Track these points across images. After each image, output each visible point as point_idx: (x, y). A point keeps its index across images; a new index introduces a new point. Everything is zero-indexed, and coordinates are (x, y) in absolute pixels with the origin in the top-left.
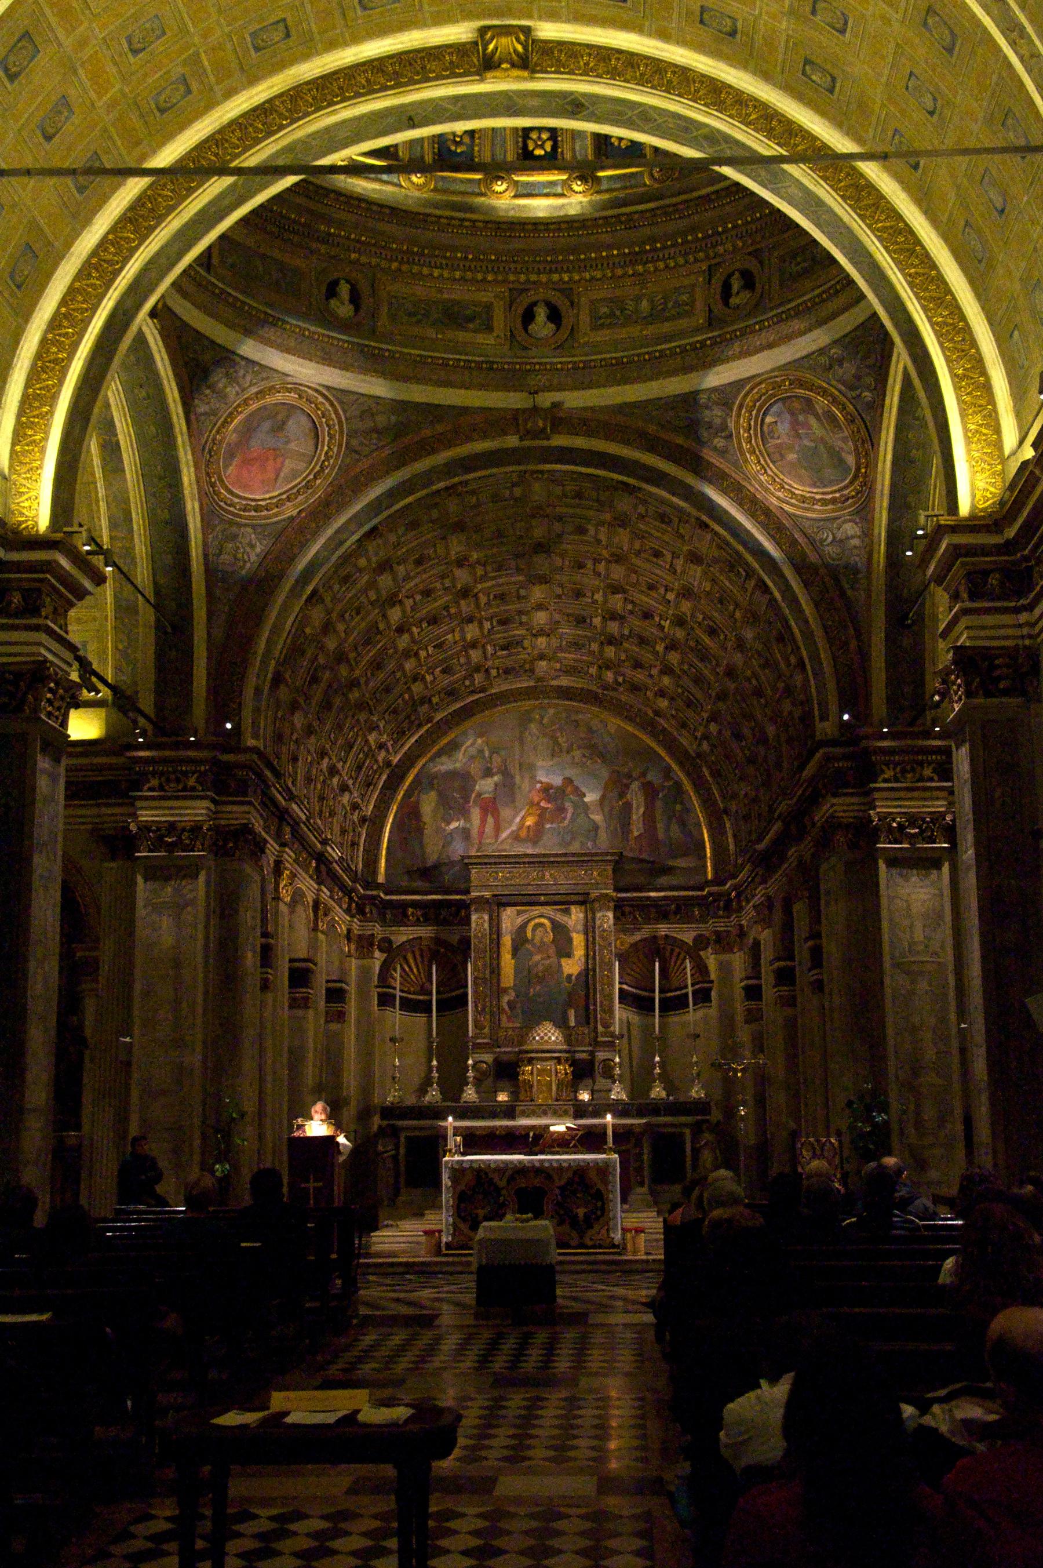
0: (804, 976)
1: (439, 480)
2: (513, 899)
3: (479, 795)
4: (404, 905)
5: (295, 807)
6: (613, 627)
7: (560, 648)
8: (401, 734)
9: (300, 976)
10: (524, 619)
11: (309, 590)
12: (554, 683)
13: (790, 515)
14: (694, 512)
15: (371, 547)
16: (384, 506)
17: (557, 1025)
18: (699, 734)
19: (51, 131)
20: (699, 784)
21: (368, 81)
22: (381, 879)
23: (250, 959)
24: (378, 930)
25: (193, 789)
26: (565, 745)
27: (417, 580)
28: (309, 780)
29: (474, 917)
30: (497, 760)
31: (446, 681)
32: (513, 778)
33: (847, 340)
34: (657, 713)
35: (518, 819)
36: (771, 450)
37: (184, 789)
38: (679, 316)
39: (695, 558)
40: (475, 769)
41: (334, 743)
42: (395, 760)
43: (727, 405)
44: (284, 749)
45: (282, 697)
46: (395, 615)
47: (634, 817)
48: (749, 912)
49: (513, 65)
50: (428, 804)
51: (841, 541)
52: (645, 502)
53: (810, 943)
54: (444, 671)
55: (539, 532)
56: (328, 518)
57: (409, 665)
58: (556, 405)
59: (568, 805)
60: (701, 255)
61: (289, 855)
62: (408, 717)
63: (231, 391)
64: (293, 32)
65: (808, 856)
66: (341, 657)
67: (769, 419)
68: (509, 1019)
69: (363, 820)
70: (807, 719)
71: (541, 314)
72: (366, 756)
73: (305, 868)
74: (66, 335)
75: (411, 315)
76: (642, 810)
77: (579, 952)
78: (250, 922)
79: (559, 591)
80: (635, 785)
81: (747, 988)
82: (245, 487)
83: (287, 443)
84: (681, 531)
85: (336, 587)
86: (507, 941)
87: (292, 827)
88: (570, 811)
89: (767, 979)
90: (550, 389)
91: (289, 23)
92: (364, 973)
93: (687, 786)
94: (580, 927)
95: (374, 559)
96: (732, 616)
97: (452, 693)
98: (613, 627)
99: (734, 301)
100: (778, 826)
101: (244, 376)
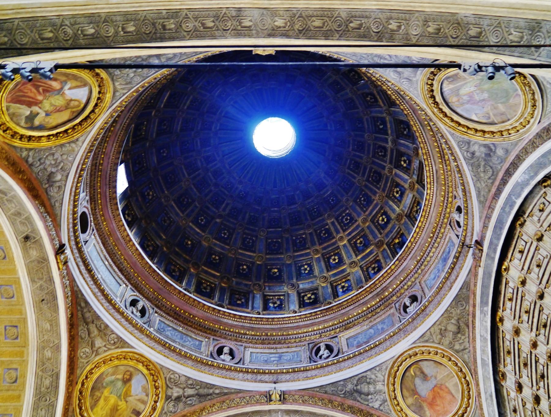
16: (486, 359)
55: (532, 288)
63: (379, 386)
64: (15, 325)
75: (434, 278)
83: (436, 378)
101: (377, 377)
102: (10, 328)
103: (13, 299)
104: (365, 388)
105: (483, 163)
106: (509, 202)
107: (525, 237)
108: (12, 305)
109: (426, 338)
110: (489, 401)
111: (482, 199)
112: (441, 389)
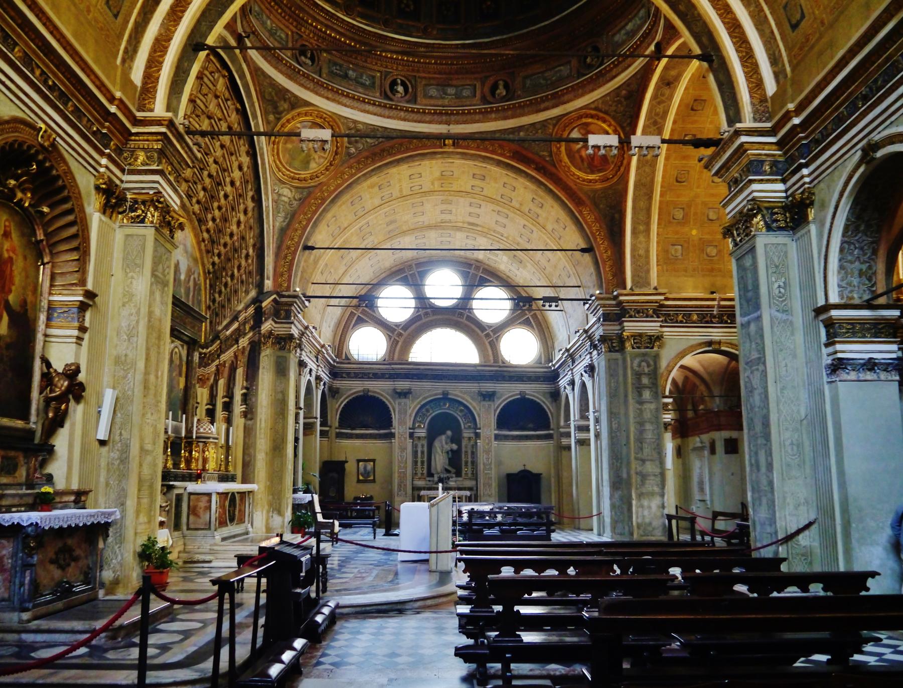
6: (207, 181)
18: (211, 260)
33: (372, 127)
39: (240, 168)
43: (293, 106)
48: (213, 368)
51: (280, 195)
60: (295, 23)
65: (245, 345)
80: (192, 277)
81: (208, 410)
100: (235, 325)
105: (275, 98)
111: (259, 73)
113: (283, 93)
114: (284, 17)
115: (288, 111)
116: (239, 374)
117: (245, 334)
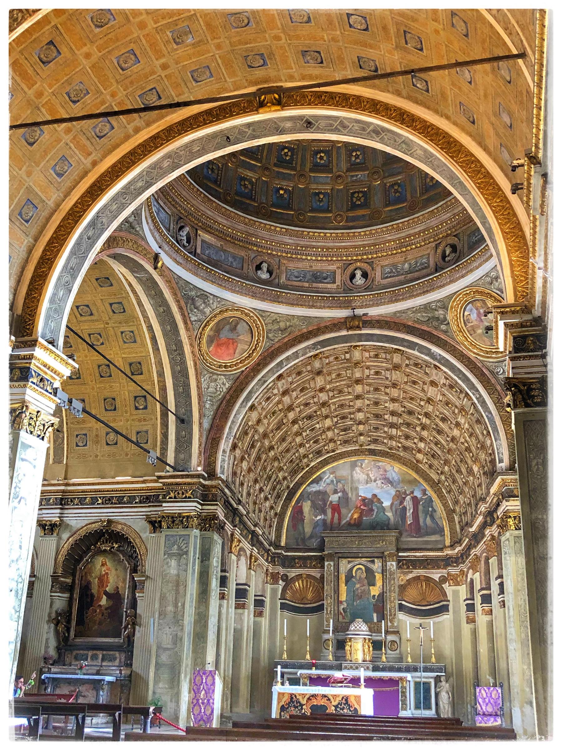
0: (496, 599)
1: (310, 352)
2: (345, 555)
3: (331, 502)
4: (294, 558)
5: (240, 507)
6: (395, 419)
7: (370, 431)
8: (294, 472)
9: (241, 593)
10: (352, 416)
11: (249, 404)
12: (368, 447)
13: (481, 361)
14: (432, 361)
15: (280, 384)
16: (285, 364)
17: (365, 622)
18: (439, 472)
19: (32, 141)
20: (441, 497)
21: (204, 119)
22: (283, 544)
23: (214, 583)
24: (282, 570)
25: (190, 498)
26: (373, 478)
27: (301, 399)
28: (249, 494)
29: (326, 563)
30: (340, 486)
31: (316, 447)
32: (347, 494)
34: (418, 461)
35: (350, 515)
36: (469, 329)
37: (186, 497)
38: (423, 269)
40: (329, 489)
41: (262, 477)
42: (291, 486)
44: (238, 479)
45: (237, 455)
46: (291, 415)
47: (408, 514)
49: (273, 104)
50: (307, 507)
52: (408, 358)
53: (499, 581)
54: (314, 442)
55: (358, 375)
56: (259, 371)
57: (298, 440)
58: (364, 315)
59: (374, 508)
61: (237, 531)
62: (298, 464)
63: (208, 310)
64: (161, 96)
65: (496, 534)
66: (265, 435)
67: (466, 313)
68: (344, 618)
69: (276, 514)
70: (493, 462)
71: (359, 273)
72: (277, 483)
73: (246, 537)
74: (55, 247)
75: (296, 277)
76: (411, 511)
77: (379, 583)
78: (215, 564)
79: (368, 402)
80: (408, 498)
81: (467, 605)
82: (219, 357)
84: (427, 371)
85: (264, 403)
86: (343, 577)
87: (240, 518)
88: (376, 510)
89: (478, 600)
90: (361, 307)
91: (159, 91)
92: (274, 591)
93: (434, 497)
94: (380, 570)
95: (281, 390)
96: (454, 412)
97: (319, 453)
98: (395, 419)
99: (447, 259)
100: (480, 519)
102: (155, 93)
103: (194, 83)
104: (199, 302)
106: (412, 345)
107: (388, 357)
108: (186, 84)
109: (264, 315)
110: (261, 383)
112: (233, 344)
113: (426, 307)
114: (421, 246)
115: (447, 313)
116: (492, 564)
117: (491, 525)
